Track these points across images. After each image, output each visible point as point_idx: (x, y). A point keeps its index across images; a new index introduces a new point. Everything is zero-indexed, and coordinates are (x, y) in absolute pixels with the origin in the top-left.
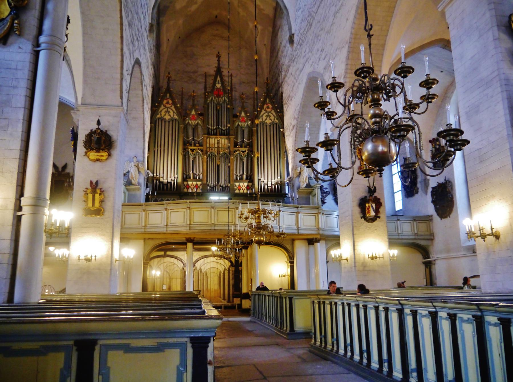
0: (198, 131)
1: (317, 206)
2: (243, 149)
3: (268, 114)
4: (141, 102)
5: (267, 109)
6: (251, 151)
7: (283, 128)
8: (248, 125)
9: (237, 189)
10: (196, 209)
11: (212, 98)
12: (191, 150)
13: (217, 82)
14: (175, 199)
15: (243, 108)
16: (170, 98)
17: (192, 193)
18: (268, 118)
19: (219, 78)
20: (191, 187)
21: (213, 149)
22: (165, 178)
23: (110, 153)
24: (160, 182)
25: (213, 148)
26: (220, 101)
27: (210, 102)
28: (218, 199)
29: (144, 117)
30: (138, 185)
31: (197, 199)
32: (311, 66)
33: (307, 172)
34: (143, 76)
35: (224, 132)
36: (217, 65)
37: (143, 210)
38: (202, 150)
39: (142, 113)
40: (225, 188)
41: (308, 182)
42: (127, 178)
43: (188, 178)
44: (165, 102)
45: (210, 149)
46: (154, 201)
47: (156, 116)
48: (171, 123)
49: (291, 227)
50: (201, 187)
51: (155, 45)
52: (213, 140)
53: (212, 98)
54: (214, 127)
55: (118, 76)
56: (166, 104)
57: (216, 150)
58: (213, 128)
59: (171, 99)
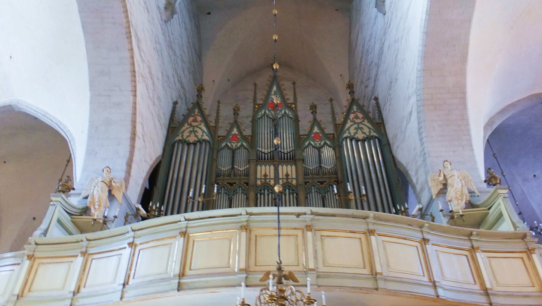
0: (241, 155)
3: (358, 125)
5: (355, 119)
11: (265, 112)
18: (359, 132)
27: (262, 116)
34: (138, 40)
35: (286, 155)
39: (131, 94)
44: (191, 119)
48: (198, 145)
49: (466, 286)
53: (265, 112)
54: (269, 150)
56: (192, 123)
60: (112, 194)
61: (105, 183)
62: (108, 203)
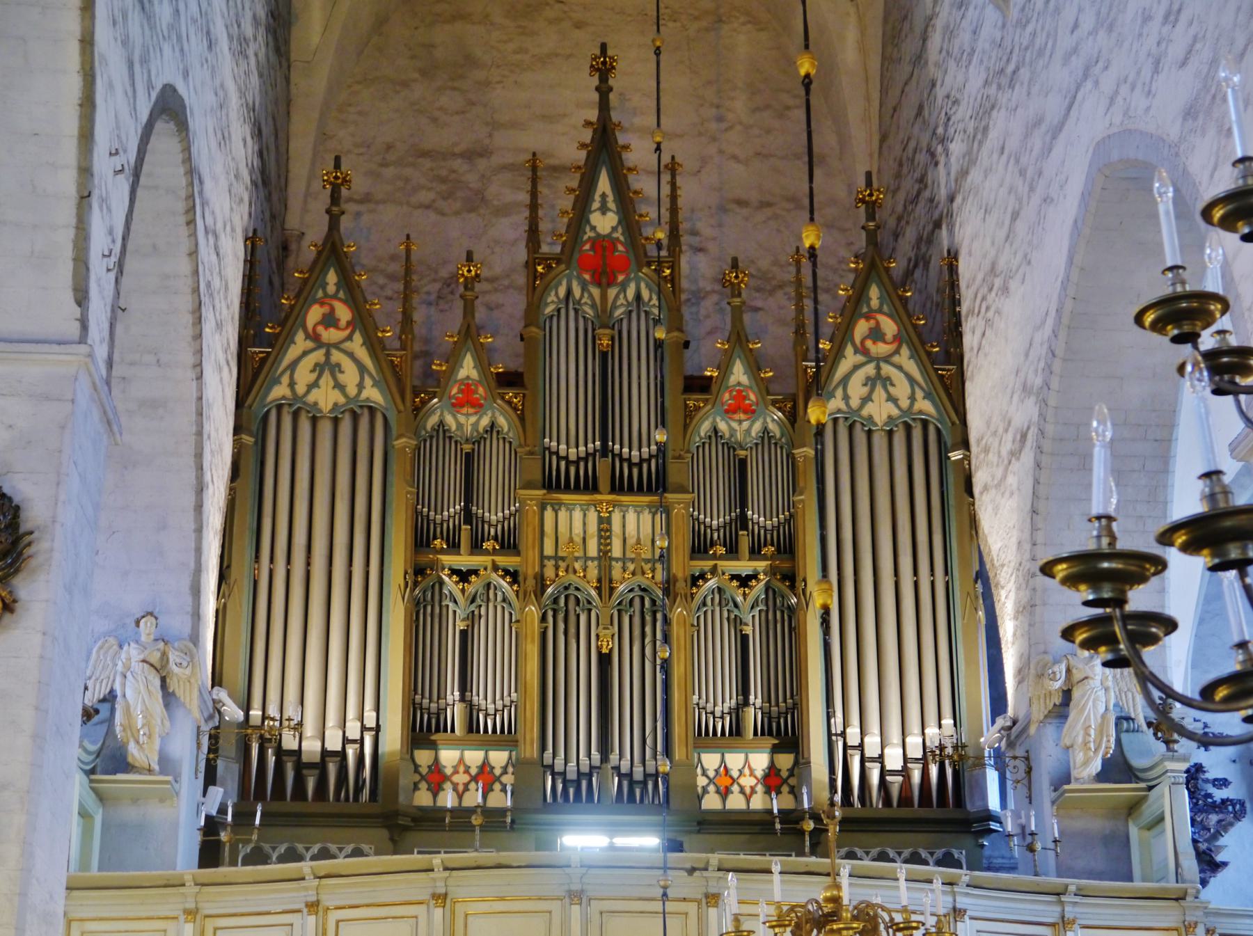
1: (1171, 884)
2: (744, 566)
3: (878, 368)
4: (188, 319)
5: (869, 343)
6: (785, 577)
7: (965, 444)
8: (765, 430)
9: (712, 788)
10: (483, 907)
11: (569, 292)
12: (454, 572)
13: (596, 205)
14: (365, 847)
15: (739, 338)
16: (341, 294)
17: (461, 816)
18: (879, 394)
19: (604, 184)
20: (456, 778)
21: (577, 565)
22: (310, 729)
23: (11, 593)
24: (280, 753)
25: (577, 559)
26: (614, 307)
28: (602, 849)
29: (200, 398)
30: (163, 771)
31: (484, 845)
32: (1112, 101)
33: (1107, 689)
34: (201, 182)
35: (635, 471)
36: (593, 115)
37: (187, 912)
38: (514, 576)
39: (191, 374)
40: (644, 783)
41: (1113, 740)
42: (104, 728)
43: (438, 730)
44: (314, 314)
45: (557, 568)
46: (245, 863)
47: (269, 390)
50: (508, 779)
51: (262, 13)
52: (577, 515)
53: (569, 292)
54: (582, 448)
55: (67, 182)
56: (320, 329)
57: (593, 572)
58: (573, 451)
59: (345, 302)
60: (171, 690)
61: (152, 665)
62: (167, 723)
